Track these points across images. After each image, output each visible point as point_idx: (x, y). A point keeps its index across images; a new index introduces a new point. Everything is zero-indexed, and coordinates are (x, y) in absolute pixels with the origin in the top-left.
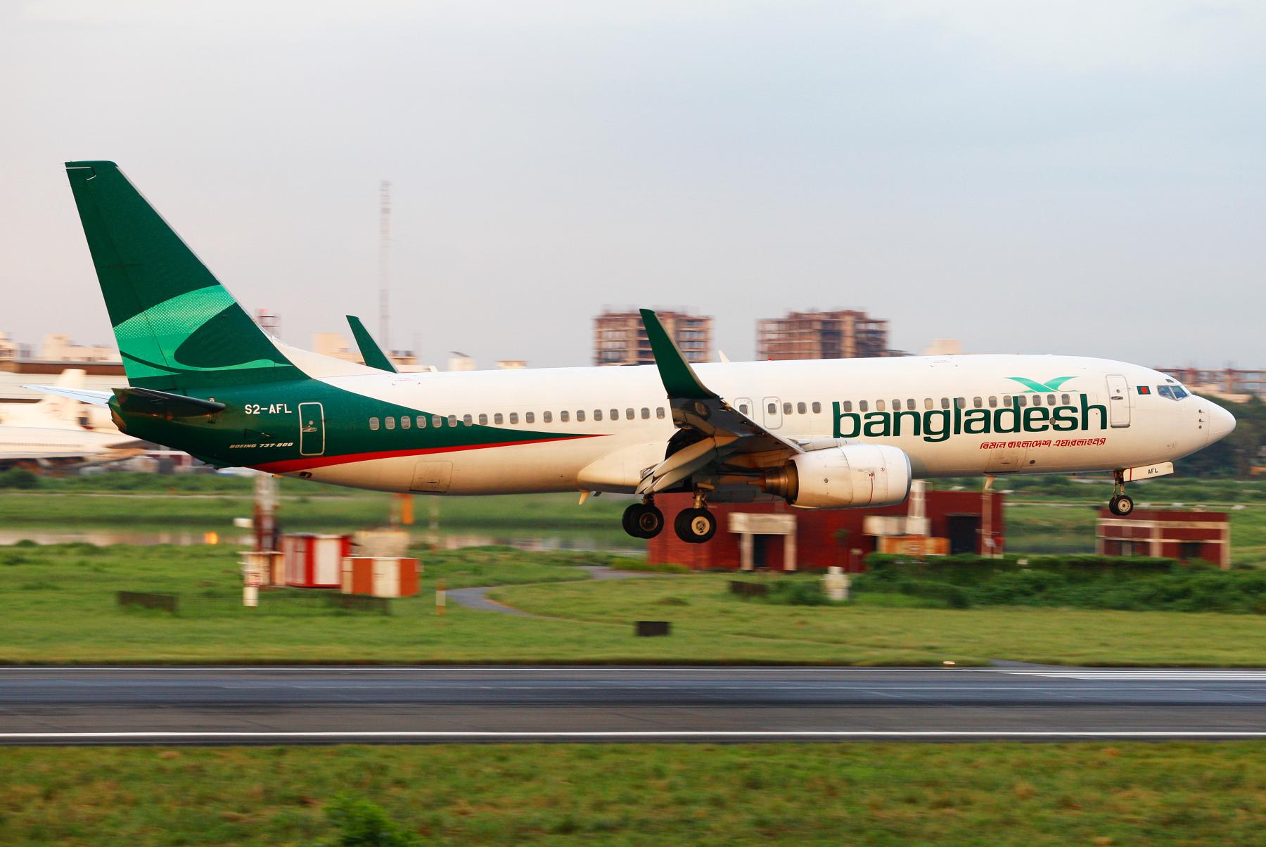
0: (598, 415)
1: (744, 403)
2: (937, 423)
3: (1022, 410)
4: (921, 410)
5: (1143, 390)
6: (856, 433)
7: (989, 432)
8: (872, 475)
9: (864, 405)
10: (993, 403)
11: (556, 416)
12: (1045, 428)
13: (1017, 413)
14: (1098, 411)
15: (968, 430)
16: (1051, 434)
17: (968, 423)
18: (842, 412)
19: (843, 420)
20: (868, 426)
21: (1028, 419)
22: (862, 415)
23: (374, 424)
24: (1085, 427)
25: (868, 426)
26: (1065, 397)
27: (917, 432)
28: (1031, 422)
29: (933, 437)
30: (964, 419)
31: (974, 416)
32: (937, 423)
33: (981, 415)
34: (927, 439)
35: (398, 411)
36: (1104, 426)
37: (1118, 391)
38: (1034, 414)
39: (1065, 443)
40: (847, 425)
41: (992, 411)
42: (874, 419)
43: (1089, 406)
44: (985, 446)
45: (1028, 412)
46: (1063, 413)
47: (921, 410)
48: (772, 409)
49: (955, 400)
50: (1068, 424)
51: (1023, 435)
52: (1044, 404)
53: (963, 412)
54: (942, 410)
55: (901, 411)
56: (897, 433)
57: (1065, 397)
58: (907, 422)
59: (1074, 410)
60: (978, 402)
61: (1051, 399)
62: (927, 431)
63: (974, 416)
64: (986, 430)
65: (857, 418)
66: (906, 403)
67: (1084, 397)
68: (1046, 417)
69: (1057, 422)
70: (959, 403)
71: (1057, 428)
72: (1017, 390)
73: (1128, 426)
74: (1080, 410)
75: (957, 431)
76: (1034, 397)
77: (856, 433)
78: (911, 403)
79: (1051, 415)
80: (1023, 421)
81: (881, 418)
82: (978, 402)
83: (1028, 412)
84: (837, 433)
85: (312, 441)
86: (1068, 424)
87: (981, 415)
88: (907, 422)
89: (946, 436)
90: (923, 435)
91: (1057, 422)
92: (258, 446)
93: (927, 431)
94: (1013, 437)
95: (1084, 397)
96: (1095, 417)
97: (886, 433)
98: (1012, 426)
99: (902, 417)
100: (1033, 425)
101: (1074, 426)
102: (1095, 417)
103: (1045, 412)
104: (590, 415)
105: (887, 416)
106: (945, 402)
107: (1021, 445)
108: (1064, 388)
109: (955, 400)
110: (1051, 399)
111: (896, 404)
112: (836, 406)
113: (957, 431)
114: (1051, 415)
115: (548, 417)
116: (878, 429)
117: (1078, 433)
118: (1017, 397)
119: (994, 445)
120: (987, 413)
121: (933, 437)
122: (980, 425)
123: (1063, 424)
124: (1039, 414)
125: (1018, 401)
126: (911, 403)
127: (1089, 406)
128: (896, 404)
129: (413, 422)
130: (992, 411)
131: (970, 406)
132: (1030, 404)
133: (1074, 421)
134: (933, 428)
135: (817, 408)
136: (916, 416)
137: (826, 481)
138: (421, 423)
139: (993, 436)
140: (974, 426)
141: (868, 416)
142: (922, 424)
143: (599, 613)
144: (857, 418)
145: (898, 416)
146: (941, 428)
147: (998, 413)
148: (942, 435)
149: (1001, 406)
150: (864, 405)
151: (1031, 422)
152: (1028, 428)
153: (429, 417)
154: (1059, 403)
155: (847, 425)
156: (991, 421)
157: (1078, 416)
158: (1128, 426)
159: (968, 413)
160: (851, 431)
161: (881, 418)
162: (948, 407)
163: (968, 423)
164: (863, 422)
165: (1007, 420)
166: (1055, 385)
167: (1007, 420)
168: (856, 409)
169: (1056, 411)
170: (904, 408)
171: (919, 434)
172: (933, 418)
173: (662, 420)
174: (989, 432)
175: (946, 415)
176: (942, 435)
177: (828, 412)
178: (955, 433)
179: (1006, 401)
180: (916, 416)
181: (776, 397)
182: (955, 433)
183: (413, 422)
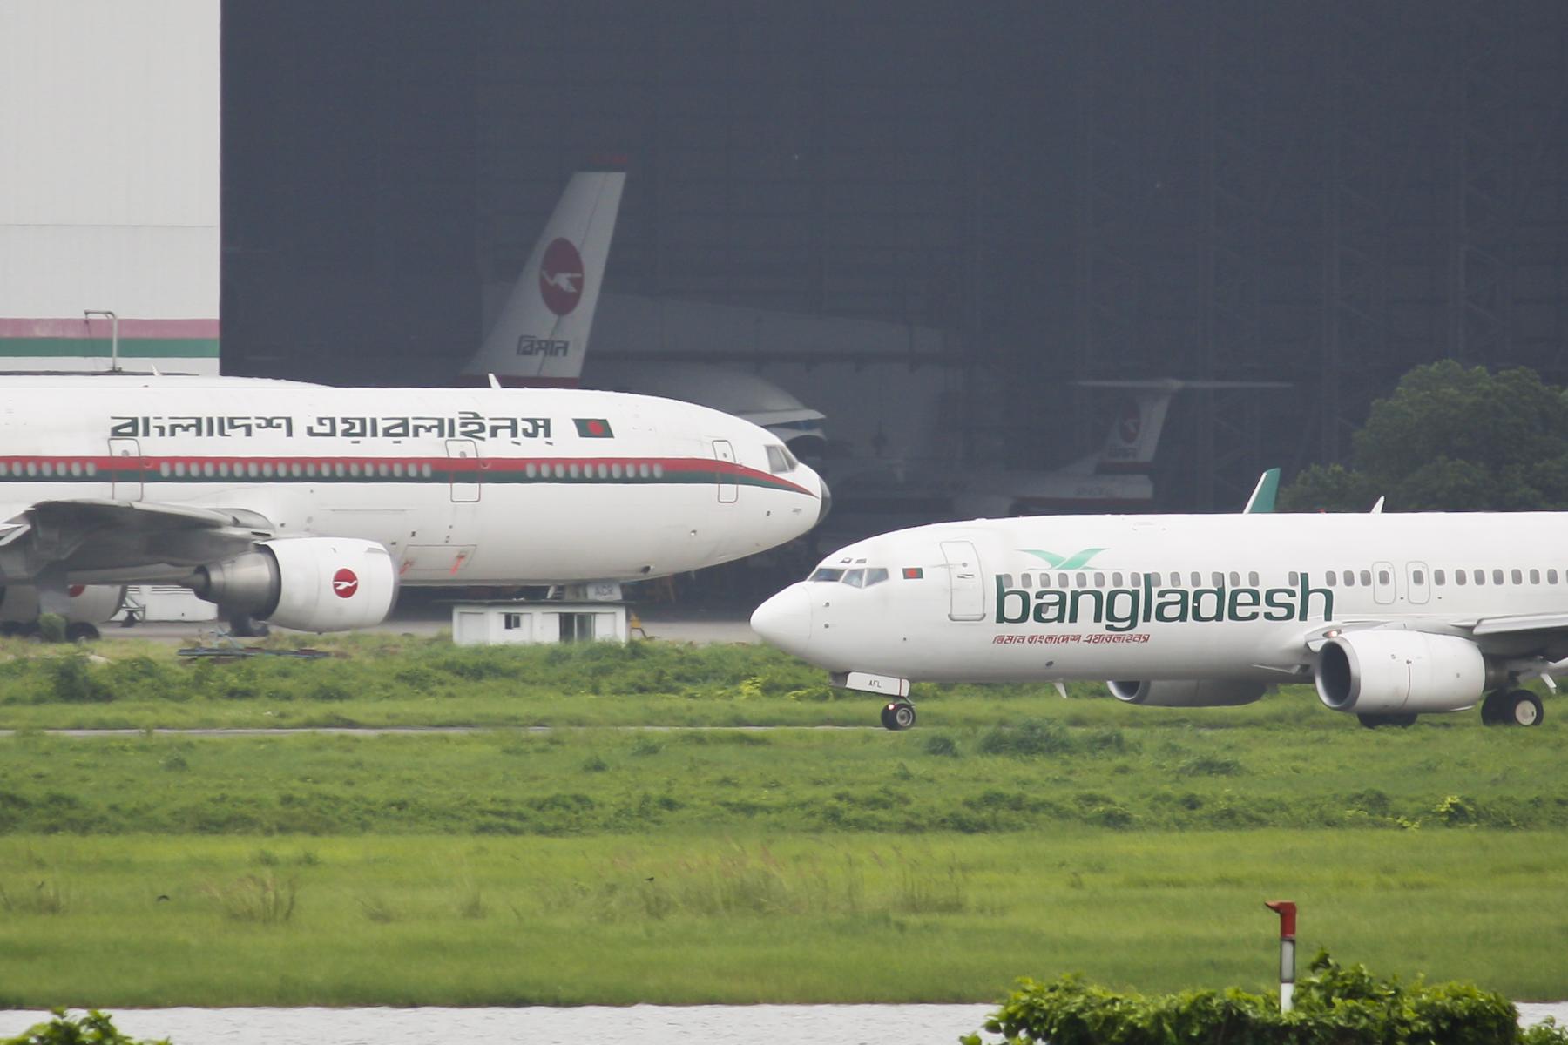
2: (1123, 606)
6: (1024, 618)
7: (1186, 620)
10: (1196, 578)
12: (1254, 616)
14: (1322, 595)
15: (1160, 617)
17: (1161, 607)
20: (1039, 609)
21: (1234, 603)
25: (1039, 609)
27: (1098, 618)
28: (1238, 608)
29: (1117, 625)
30: (1156, 601)
32: (1123, 606)
33: (1178, 597)
34: (1109, 628)
41: (1191, 592)
43: (1310, 589)
45: (1234, 594)
50: (1283, 612)
53: (1155, 591)
54: (1130, 589)
56: (1073, 619)
58: (1087, 604)
59: (1292, 594)
60: (1175, 577)
62: (1111, 617)
63: (1169, 598)
65: (1025, 598)
66: (1454, 575)
68: (1256, 602)
71: (1268, 616)
75: (1147, 618)
77: (1024, 618)
80: (1228, 606)
82: (1175, 577)
86: (1283, 612)
88: (1087, 604)
89: (1133, 625)
90: (1105, 621)
93: (1111, 617)
96: (1318, 602)
97: (1060, 618)
98: (1214, 613)
99: (1311, 596)
100: (1242, 611)
101: (1290, 616)
102: (1318, 602)
103: (1255, 595)
106: (1135, 578)
107: (1043, 641)
113: (1147, 618)
118: (1149, 575)
120: (1184, 594)
121: (1117, 625)
124: (1247, 598)
127: (1310, 589)
131: (1166, 584)
133: (1290, 608)
134: (1117, 614)
136: (1098, 596)
142: (1104, 607)
143: (873, 803)
144: (1025, 598)
145: (1076, 596)
146: (1127, 613)
147: (1198, 596)
148: (1128, 623)
151: (1238, 608)
152: (1233, 616)
155: (1013, 607)
156: (1189, 607)
157: (1296, 602)
159: (1161, 594)
160: (1018, 615)
162: (1139, 584)
163: (1161, 607)
164: (1034, 602)
165: (1208, 605)
167: (1208, 605)
171: (1100, 621)
172: (1119, 598)
173: (1499, 586)
174: (1186, 620)
175: (1135, 595)
176: (1128, 623)
180: (1098, 596)
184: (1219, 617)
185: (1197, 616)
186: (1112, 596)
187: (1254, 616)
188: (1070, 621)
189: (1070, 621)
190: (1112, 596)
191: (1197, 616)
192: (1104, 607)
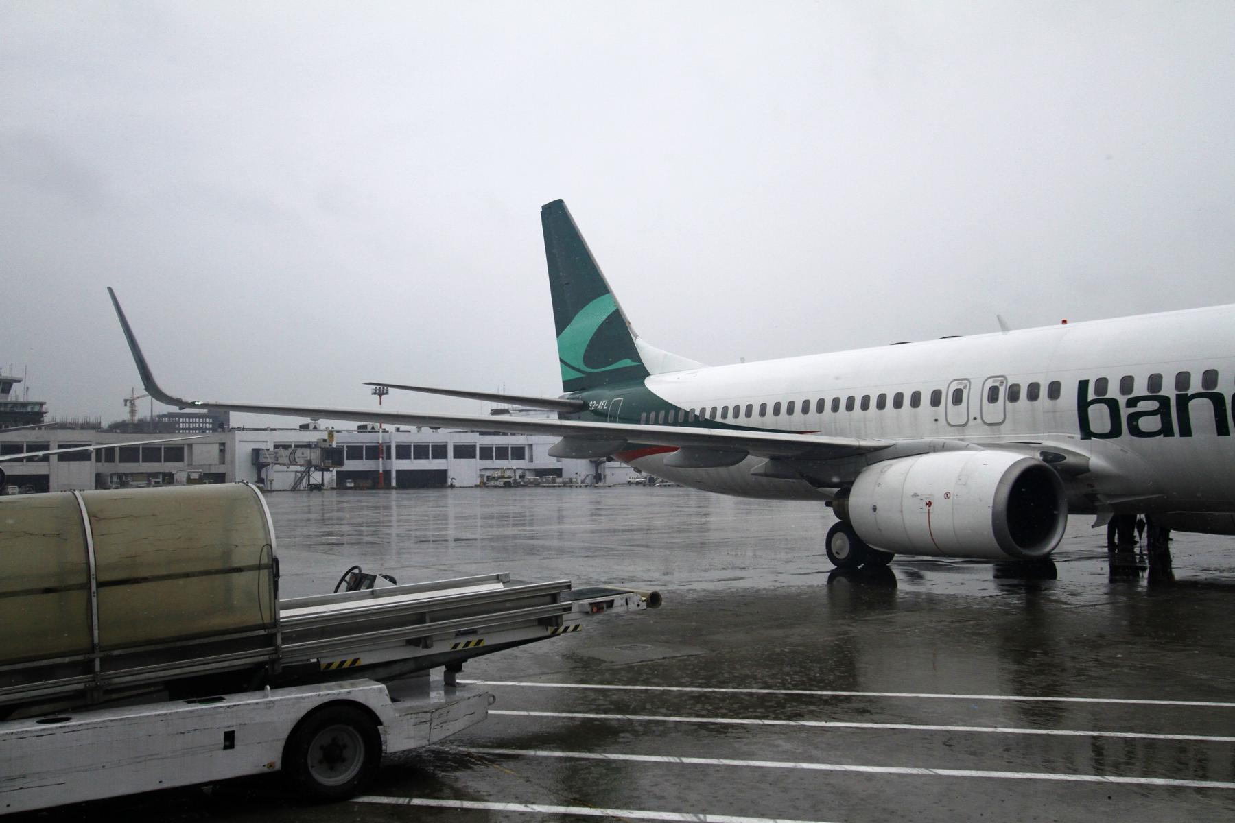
6: (1115, 432)
8: (929, 504)
18: (1091, 396)
19: (1091, 409)
22: (1122, 400)
42: (1142, 406)
48: (993, 395)
55: (1190, 392)
56: (1186, 431)
81: (1153, 405)
97: (1166, 430)
105: (1164, 401)
112: (1083, 385)
116: (1150, 424)
135: (1055, 390)
137: (875, 509)
141: (1132, 403)
145: (1183, 401)
155: (1099, 417)
161: (1153, 405)
164: (1125, 412)
168: (1113, 392)
170: (1196, 386)
181: (1002, 376)
188: (1182, 434)
189: (1182, 434)
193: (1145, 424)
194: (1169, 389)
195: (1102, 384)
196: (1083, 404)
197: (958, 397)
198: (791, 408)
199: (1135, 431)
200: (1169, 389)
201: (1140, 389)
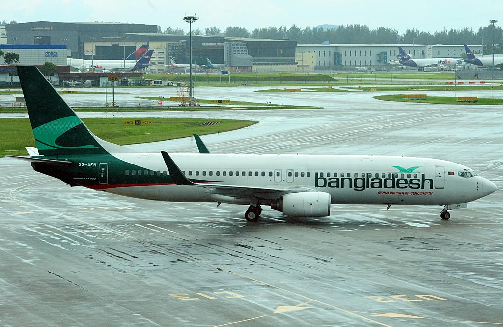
0: (218, 174)
1: (278, 171)
2: (359, 183)
3: (396, 179)
4: (353, 177)
5: (451, 173)
6: (325, 186)
9: (328, 175)
11: (201, 173)
12: (406, 187)
13: (393, 180)
15: (372, 186)
16: (408, 190)
17: (372, 184)
18: (319, 177)
20: (330, 183)
21: (398, 183)
22: (327, 178)
23: (127, 172)
24: (423, 187)
25: (330, 183)
26: (415, 176)
27: (351, 186)
29: (358, 188)
30: (371, 182)
31: (375, 181)
33: (378, 181)
35: (137, 168)
36: (432, 187)
37: (439, 174)
38: (401, 181)
39: (414, 194)
40: (321, 182)
41: (383, 179)
42: (332, 180)
44: (380, 193)
45: (398, 180)
46: (413, 181)
47: (353, 178)
48: (290, 174)
49: (367, 174)
50: (416, 186)
51: (396, 189)
52: (406, 177)
56: (342, 186)
57: (415, 176)
58: (347, 182)
59: (419, 180)
60: (377, 175)
61: (409, 176)
62: (355, 186)
63: (375, 181)
64: (380, 187)
67: (423, 176)
69: (411, 185)
70: (369, 176)
71: (411, 187)
72: (395, 171)
73: (443, 188)
74: (421, 180)
76: (402, 174)
77: (325, 186)
78: (349, 175)
79: (408, 182)
81: (336, 180)
82: (377, 175)
83: (398, 180)
84: (317, 185)
85: (104, 180)
86: (416, 186)
87: (378, 181)
88: (347, 182)
89: (364, 188)
90: (353, 187)
91: (411, 185)
92: (83, 178)
93: (355, 186)
94: (392, 190)
95: (423, 176)
96: (428, 184)
97: (338, 186)
101: (419, 187)
102: (428, 184)
103: (406, 180)
104: (214, 174)
105: (338, 179)
106: (363, 176)
108: (415, 172)
109: (367, 174)
110: (409, 176)
111: (342, 175)
112: (317, 174)
114: (408, 182)
115: (197, 173)
117: (420, 190)
119: (384, 193)
121: (358, 188)
122: (378, 185)
123: (413, 186)
125: (394, 176)
126: (349, 175)
128: (342, 175)
129: (143, 173)
130: (383, 179)
132: (399, 177)
133: (419, 185)
135: (309, 175)
138: (146, 173)
139: (383, 189)
140: (375, 185)
141: (330, 179)
144: (325, 179)
145: (343, 180)
147: (386, 180)
148: (362, 188)
149: (387, 177)
150: (328, 175)
152: (398, 187)
153: (149, 171)
154: (412, 177)
155: (321, 182)
156: (382, 183)
157: (421, 183)
158: (443, 188)
159: (373, 180)
161: (336, 180)
163: (372, 184)
164: (328, 181)
165: (389, 183)
166: (411, 170)
167: (389, 183)
168: (325, 176)
169: (411, 180)
170: (345, 176)
175: (363, 180)
176: (362, 188)
177: (313, 176)
178: (367, 187)
179: (390, 175)
180: (351, 180)
182: (367, 187)
183: (143, 173)
184: (393, 187)
185: (385, 186)
186: (356, 180)
187: (406, 187)
190: (356, 180)
191: (385, 186)
192: (353, 183)
193: (332, 184)
194: (339, 177)
195: (322, 174)
196: (317, 179)
197: (278, 174)
198: (211, 174)
199: (330, 186)
200: (339, 177)
201: (332, 176)
